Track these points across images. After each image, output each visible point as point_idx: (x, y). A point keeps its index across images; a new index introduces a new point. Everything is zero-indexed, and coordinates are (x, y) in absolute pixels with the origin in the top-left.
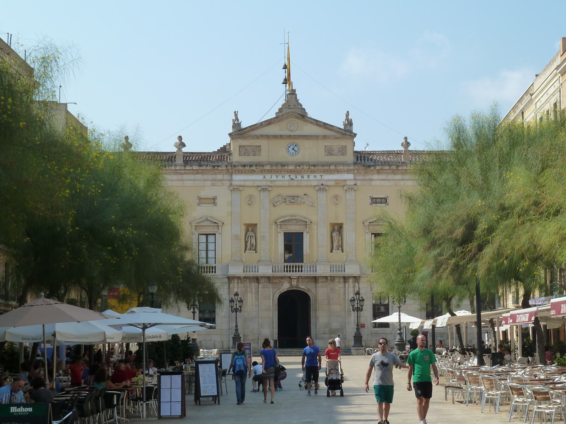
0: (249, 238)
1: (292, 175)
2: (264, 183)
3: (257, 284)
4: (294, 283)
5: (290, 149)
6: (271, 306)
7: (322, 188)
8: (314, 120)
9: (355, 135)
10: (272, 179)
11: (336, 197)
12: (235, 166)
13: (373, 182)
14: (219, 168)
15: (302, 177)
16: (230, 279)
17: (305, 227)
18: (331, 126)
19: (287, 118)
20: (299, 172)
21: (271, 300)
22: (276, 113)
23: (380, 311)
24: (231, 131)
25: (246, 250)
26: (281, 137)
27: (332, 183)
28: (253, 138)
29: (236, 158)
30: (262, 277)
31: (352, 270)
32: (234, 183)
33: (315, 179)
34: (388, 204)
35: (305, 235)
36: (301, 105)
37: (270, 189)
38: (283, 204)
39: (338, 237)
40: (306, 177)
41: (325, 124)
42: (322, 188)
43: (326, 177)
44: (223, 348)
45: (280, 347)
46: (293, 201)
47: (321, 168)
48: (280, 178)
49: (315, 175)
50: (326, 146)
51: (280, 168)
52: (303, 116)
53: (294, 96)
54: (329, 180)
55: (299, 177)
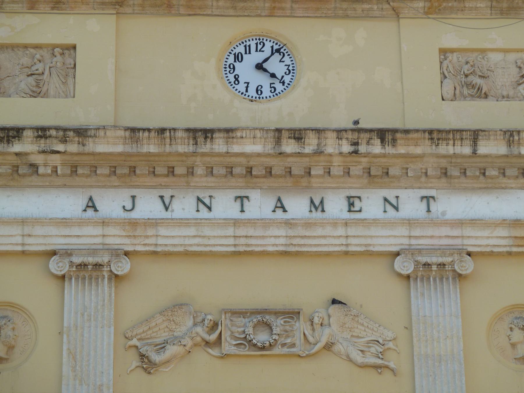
1: (255, 195)
2: (89, 236)
5: (246, 70)
7: (435, 270)
15: (318, 206)
27: (496, 240)
33: (394, 215)
37: (123, 267)
38: (203, 359)
40: (336, 206)
42: (435, 270)
43: (455, 205)
47: (424, 148)
48: (184, 206)
49: (390, 194)
50: (444, 52)
51: (183, 147)
54: (473, 222)
55: (298, 206)
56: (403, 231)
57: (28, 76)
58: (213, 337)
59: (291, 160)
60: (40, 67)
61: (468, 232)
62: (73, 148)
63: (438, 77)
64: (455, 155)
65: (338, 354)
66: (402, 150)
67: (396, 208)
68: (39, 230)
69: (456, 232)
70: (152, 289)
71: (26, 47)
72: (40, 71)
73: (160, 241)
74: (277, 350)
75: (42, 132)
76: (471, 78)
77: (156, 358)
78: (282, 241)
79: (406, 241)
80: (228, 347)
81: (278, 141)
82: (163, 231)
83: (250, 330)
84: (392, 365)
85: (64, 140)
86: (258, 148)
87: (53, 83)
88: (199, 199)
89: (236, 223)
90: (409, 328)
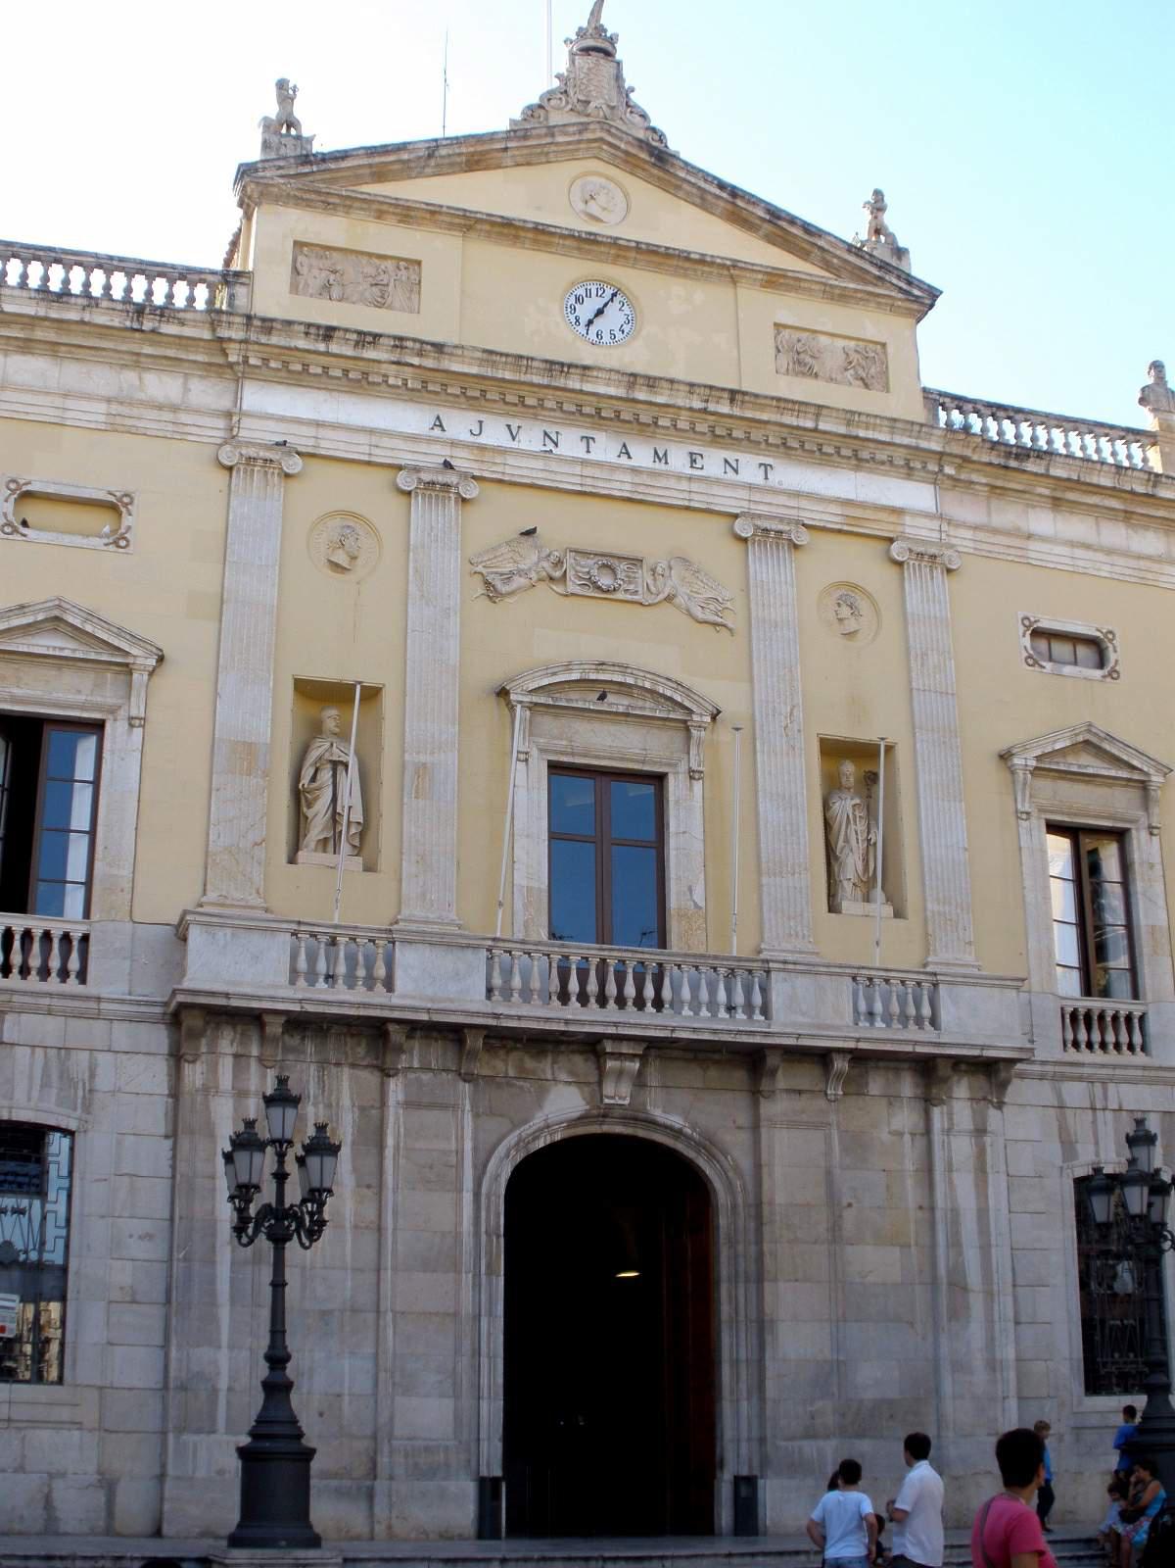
0: (326, 775)
3: (370, 1078)
4: (617, 1093)
6: (467, 1241)
8: (722, 185)
9: (933, 294)
10: (482, 440)
11: (848, 596)
12: (268, 325)
13: (1033, 545)
14: (169, 329)
16: (193, 1022)
17: (678, 737)
18: (807, 228)
19: (570, 153)
20: (645, 428)
21: (468, 1197)
22: (513, 122)
23: (1118, 1286)
24: (254, 154)
25: (296, 846)
26: (541, 236)
27: (829, 516)
28: (380, 215)
29: (272, 297)
30: (414, 1028)
31: (970, 1022)
32: (250, 430)
34: (1114, 674)
35: (675, 787)
36: (644, 116)
37: (471, 490)
38: (545, 593)
39: (861, 826)
40: (678, 460)
41: (775, 214)
42: (773, 537)
43: (793, 476)
44: (110, 1531)
45: (519, 1528)
46: (605, 581)
48: (531, 438)
49: (731, 456)
52: (654, 159)
53: (607, 68)
55: (642, 455)
56: (743, 494)
57: (372, 285)
58: (558, 574)
59: (634, 408)
60: (385, 278)
61: (804, 504)
62: (429, 363)
63: (773, 351)
64: (798, 428)
65: (678, 607)
66: (749, 414)
67: (736, 471)
68: (386, 442)
69: (792, 503)
70: (497, 518)
71: (370, 255)
72: (385, 282)
73: (508, 470)
74: (620, 595)
75: (400, 342)
76: (802, 356)
77: (504, 589)
78: (628, 487)
79: (745, 504)
80: (572, 586)
81: (631, 386)
82: (511, 460)
83: (594, 572)
84: (730, 625)
85: (420, 354)
86: (612, 391)
87: (397, 296)
88: (546, 434)
89: (584, 462)
90: (746, 590)
